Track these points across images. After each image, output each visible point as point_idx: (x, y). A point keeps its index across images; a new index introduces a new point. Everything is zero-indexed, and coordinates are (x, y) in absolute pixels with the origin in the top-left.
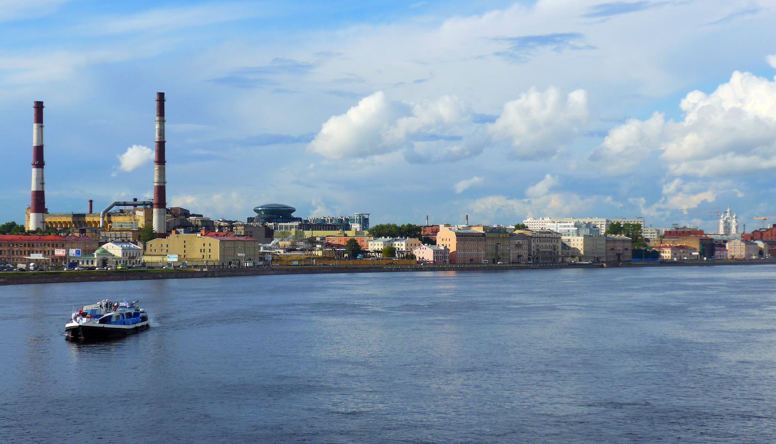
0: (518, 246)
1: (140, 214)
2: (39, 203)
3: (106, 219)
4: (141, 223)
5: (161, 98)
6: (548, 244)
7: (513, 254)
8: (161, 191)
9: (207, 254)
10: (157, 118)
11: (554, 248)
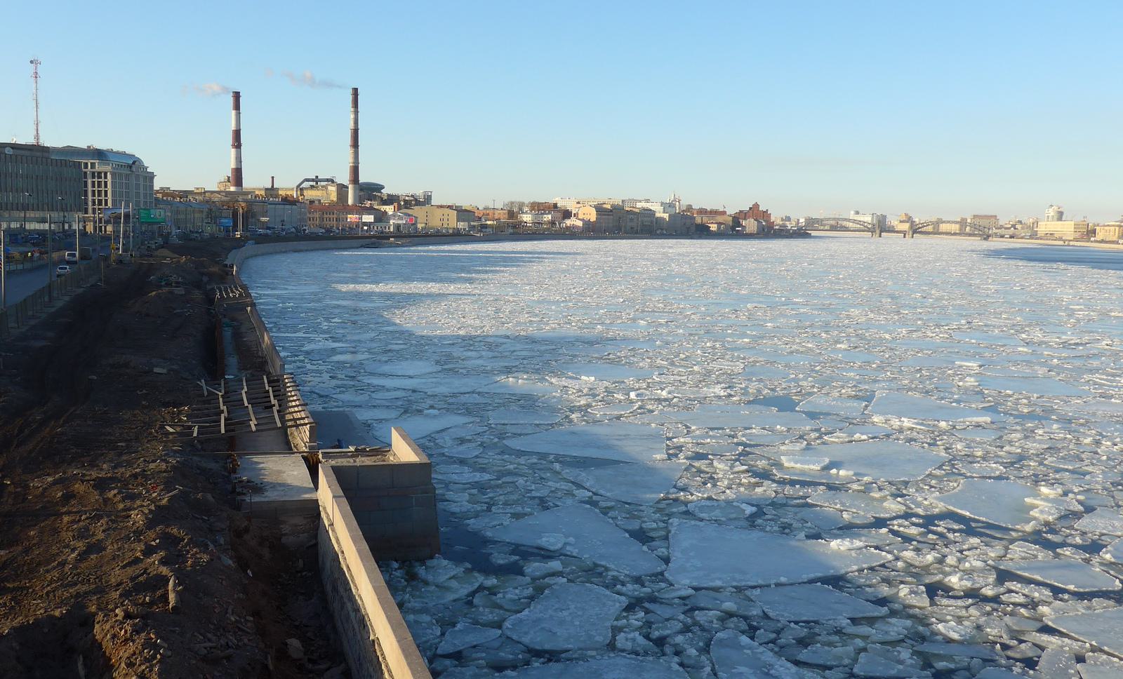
0: (632, 220)
1: (332, 189)
2: (238, 175)
3: (299, 193)
4: (334, 197)
5: (355, 91)
6: (649, 219)
7: (630, 224)
8: (355, 170)
9: (445, 222)
10: (352, 110)
11: (652, 222)
